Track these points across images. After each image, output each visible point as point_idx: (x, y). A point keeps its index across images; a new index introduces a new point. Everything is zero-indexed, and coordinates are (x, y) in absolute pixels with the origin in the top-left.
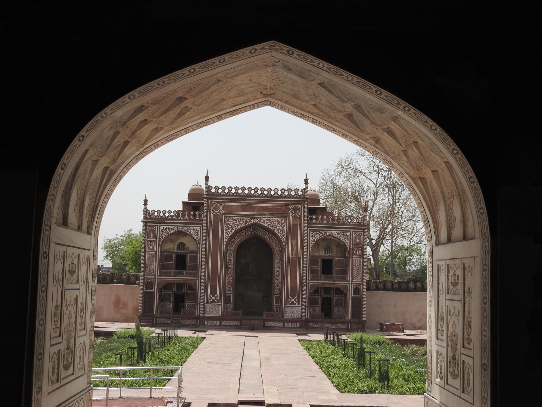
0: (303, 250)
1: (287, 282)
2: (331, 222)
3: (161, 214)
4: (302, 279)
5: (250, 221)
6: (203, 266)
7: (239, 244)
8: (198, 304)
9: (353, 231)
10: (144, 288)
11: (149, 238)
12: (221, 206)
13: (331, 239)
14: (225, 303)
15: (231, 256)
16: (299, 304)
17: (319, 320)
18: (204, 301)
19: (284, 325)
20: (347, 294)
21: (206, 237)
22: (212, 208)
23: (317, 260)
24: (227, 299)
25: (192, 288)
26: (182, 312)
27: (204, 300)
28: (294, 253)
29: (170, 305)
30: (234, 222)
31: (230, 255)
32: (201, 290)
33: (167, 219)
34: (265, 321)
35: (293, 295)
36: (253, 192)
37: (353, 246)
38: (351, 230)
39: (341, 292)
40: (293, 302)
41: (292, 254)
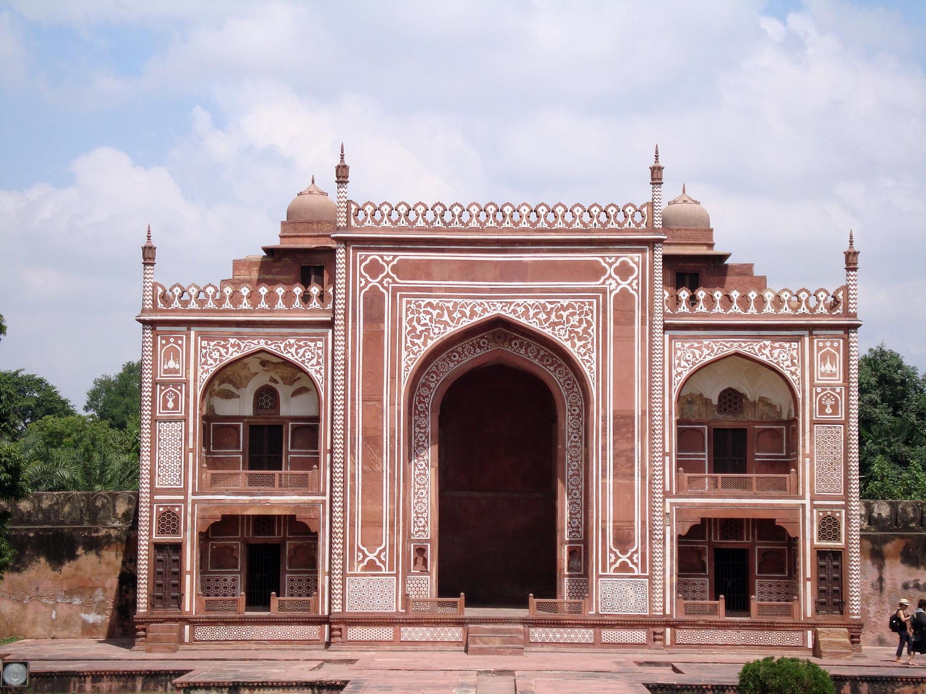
14: (407, 572)
16: (644, 571)
19: (597, 637)
20: (796, 539)
23: (701, 432)
29: (235, 581)
30: (435, 313)
35: (623, 541)
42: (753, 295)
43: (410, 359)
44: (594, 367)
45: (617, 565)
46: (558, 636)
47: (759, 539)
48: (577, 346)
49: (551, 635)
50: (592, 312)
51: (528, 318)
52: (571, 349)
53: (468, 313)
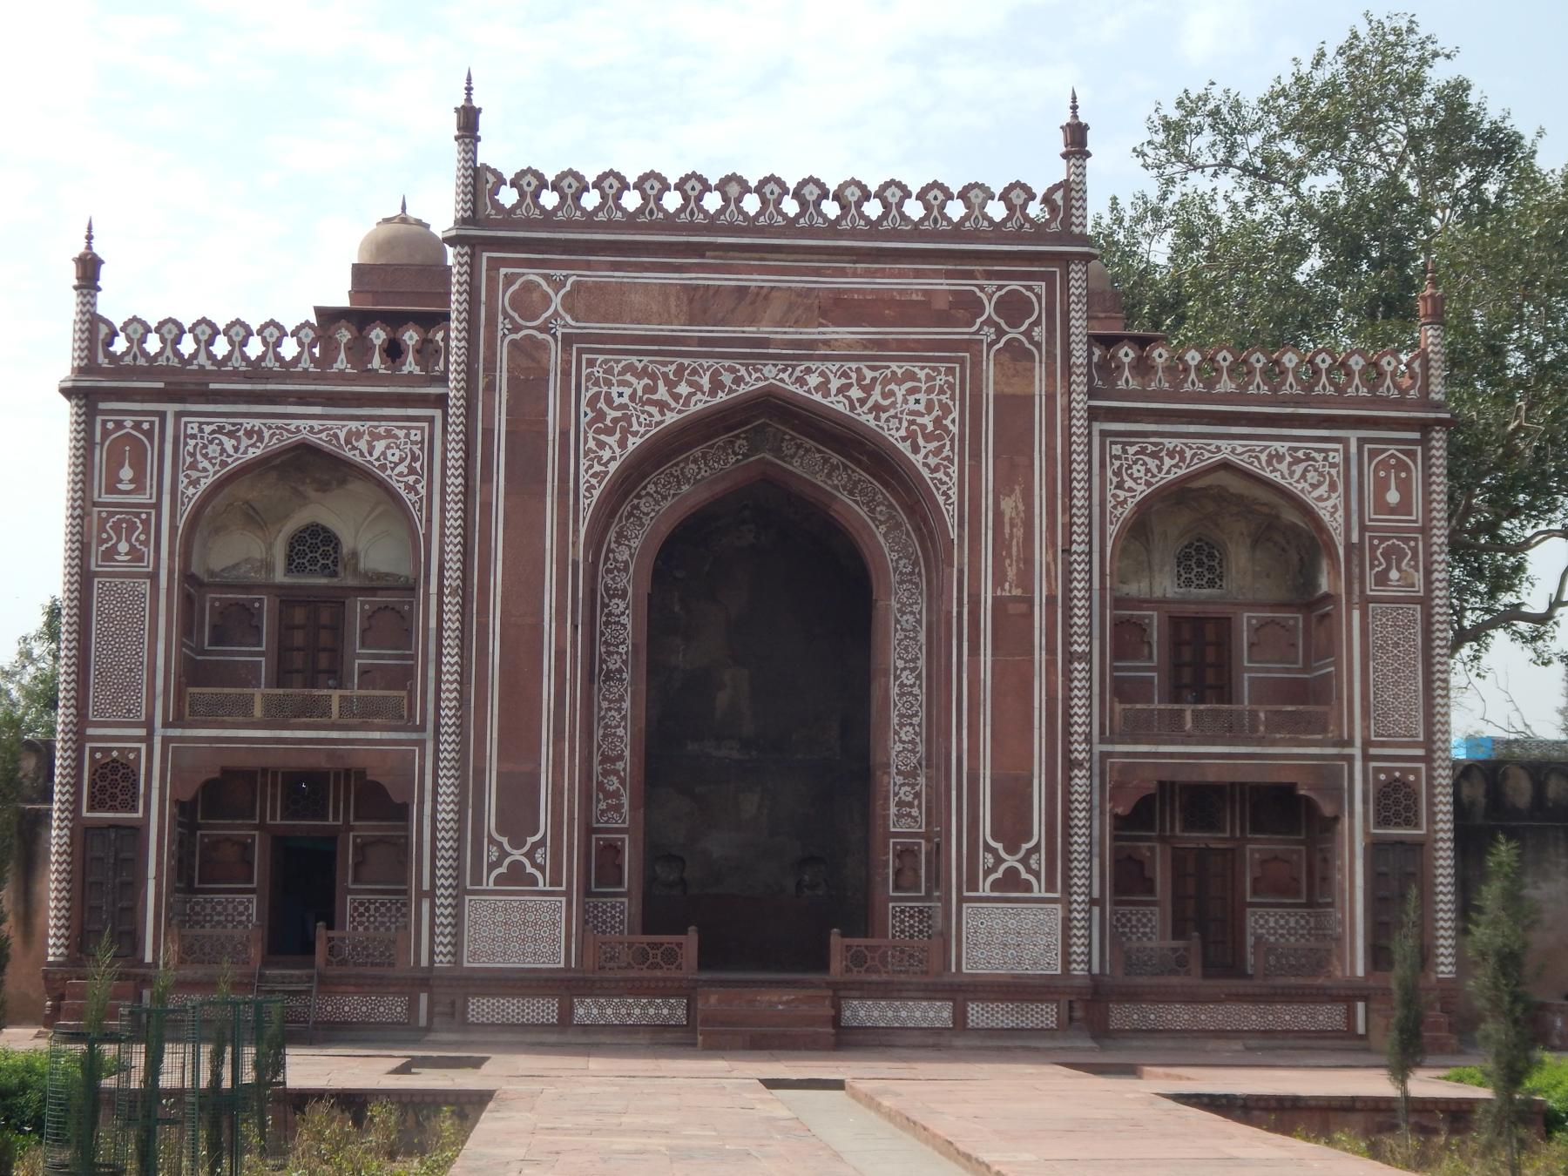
0: (1067, 551)
1: (976, 749)
2: (1226, 385)
3: (187, 346)
4: (1067, 733)
5: (738, 380)
6: (451, 659)
7: (665, 530)
8: (421, 894)
9: (1362, 442)
10: (77, 802)
11: (112, 489)
12: (554, 287)
13: (1221, 497)
15: (617, 605)
16: (1051, 887)
17: (1175, 980)
18: (459, 877)
19: (960, 1017)
21: (468, 476)
22: (504, 299)
23: (1139, 627)
24: (601, 865)
25: (383, 801)
26: (321, 948)
27: (459, 869)
28: (1011, 573)
31: (612, 593)
32: (436, 808)
33: (220, 375)
34: (840, 992)
35: (1012, 829)
36: (751, 204)
37: (1363, 528)
38: (1353, 435)
39: (1291, 811)
40: (1011, 872)
41: (999, 580)
42: (1258, 360)
43: (594, 475)
44: (954, 493)
45: (999, 875)
46: (876, 1014)
47: (1255, 830)
48: (923, 452)
49: (862, 1013)
50: (952, 387)
51: (827, 394)
52: (912, 457)
53: (706, 387)
